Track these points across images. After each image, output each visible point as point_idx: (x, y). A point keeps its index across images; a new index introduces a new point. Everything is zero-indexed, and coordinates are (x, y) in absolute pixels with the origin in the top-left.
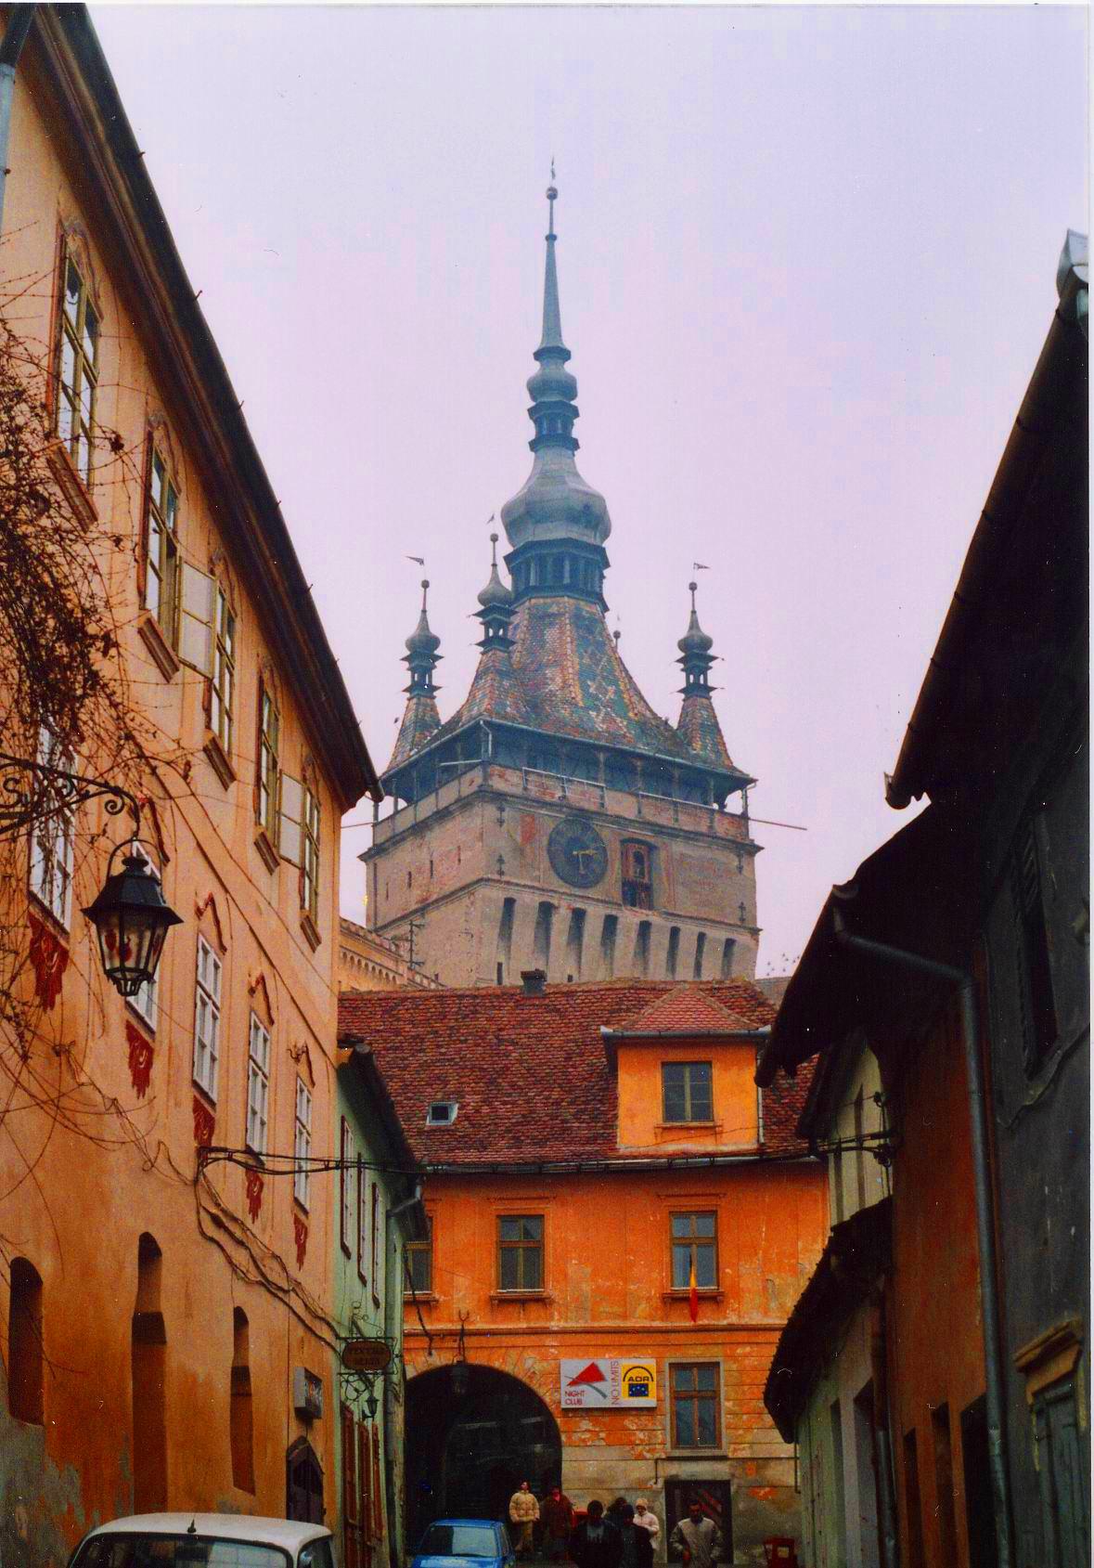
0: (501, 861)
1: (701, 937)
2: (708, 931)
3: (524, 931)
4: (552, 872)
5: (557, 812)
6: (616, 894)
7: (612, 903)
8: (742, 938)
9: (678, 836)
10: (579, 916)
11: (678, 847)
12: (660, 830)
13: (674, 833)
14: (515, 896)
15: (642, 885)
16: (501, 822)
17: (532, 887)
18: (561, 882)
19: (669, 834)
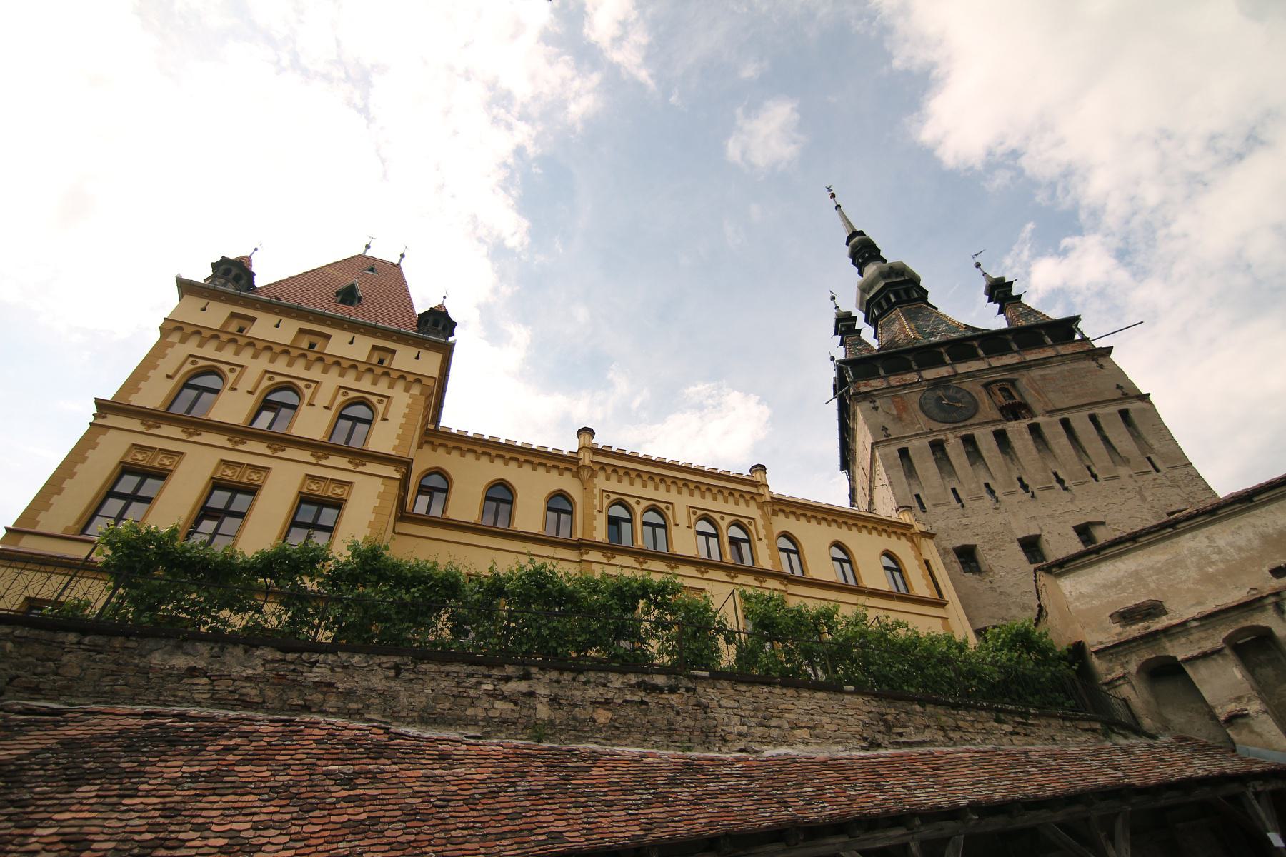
0: (884, 429)
1: (1093, 418)
2: (1099, 411)
3: (926, 465)
4: (931, 421)
5: (918, 387)
6: (997, 415)
7: (994, 421)
8: (1134, 406)
9: (1030, 367)
10: (969, 441)
11: (1036, 373)
12: (1010, 368)
13: (1026, 366)
14: (905, 445)
15: (1014, 404)
16: (876, 408)
17: (917, 435)
18: (941, 424)
19: (1023, 368)
